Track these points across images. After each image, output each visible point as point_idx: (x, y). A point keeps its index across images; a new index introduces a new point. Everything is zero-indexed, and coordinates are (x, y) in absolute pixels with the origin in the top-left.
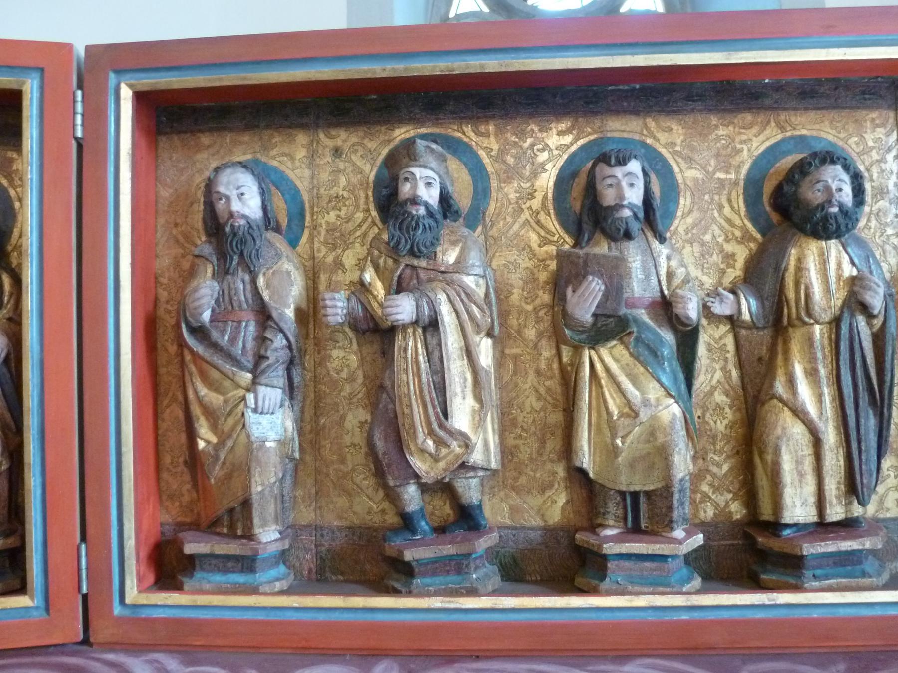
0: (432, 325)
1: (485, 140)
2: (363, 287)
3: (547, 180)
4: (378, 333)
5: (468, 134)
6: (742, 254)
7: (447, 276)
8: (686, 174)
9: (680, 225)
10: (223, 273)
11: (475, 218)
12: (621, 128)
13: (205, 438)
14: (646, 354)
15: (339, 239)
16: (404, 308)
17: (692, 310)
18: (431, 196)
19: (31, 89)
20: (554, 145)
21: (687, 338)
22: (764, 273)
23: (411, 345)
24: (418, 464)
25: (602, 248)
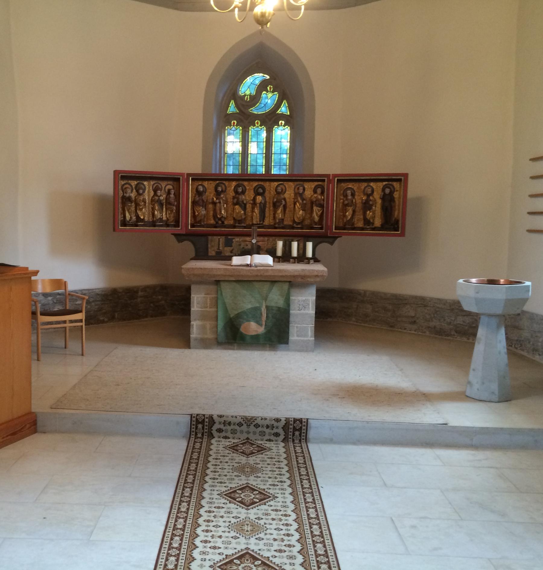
0: (220, 202)
1: (227, 183)
2: (213, 199)
3: (233, 188)
4: (214, 203)
5: (224, 182)
6: (253, 196)
7: (222, 198)
8: (247, 188)
9: (246, 193)
10: (199, 197)
11: (225, 191)
12: (241, 182)
13: (197, 214)
14: (241, 206)
15: (210, 193)
16: (218, 201)
17: (245, 202)
18: (220, 190)
19: (181, 178)
20: (234, 184)
21: (245, 205)
22: (254, 199)
23: (218, 205)
24: (218, 216)
25: (237, 196)
